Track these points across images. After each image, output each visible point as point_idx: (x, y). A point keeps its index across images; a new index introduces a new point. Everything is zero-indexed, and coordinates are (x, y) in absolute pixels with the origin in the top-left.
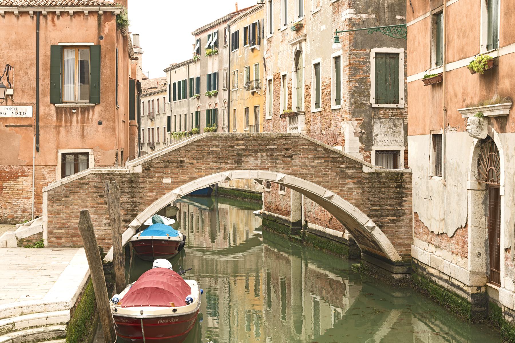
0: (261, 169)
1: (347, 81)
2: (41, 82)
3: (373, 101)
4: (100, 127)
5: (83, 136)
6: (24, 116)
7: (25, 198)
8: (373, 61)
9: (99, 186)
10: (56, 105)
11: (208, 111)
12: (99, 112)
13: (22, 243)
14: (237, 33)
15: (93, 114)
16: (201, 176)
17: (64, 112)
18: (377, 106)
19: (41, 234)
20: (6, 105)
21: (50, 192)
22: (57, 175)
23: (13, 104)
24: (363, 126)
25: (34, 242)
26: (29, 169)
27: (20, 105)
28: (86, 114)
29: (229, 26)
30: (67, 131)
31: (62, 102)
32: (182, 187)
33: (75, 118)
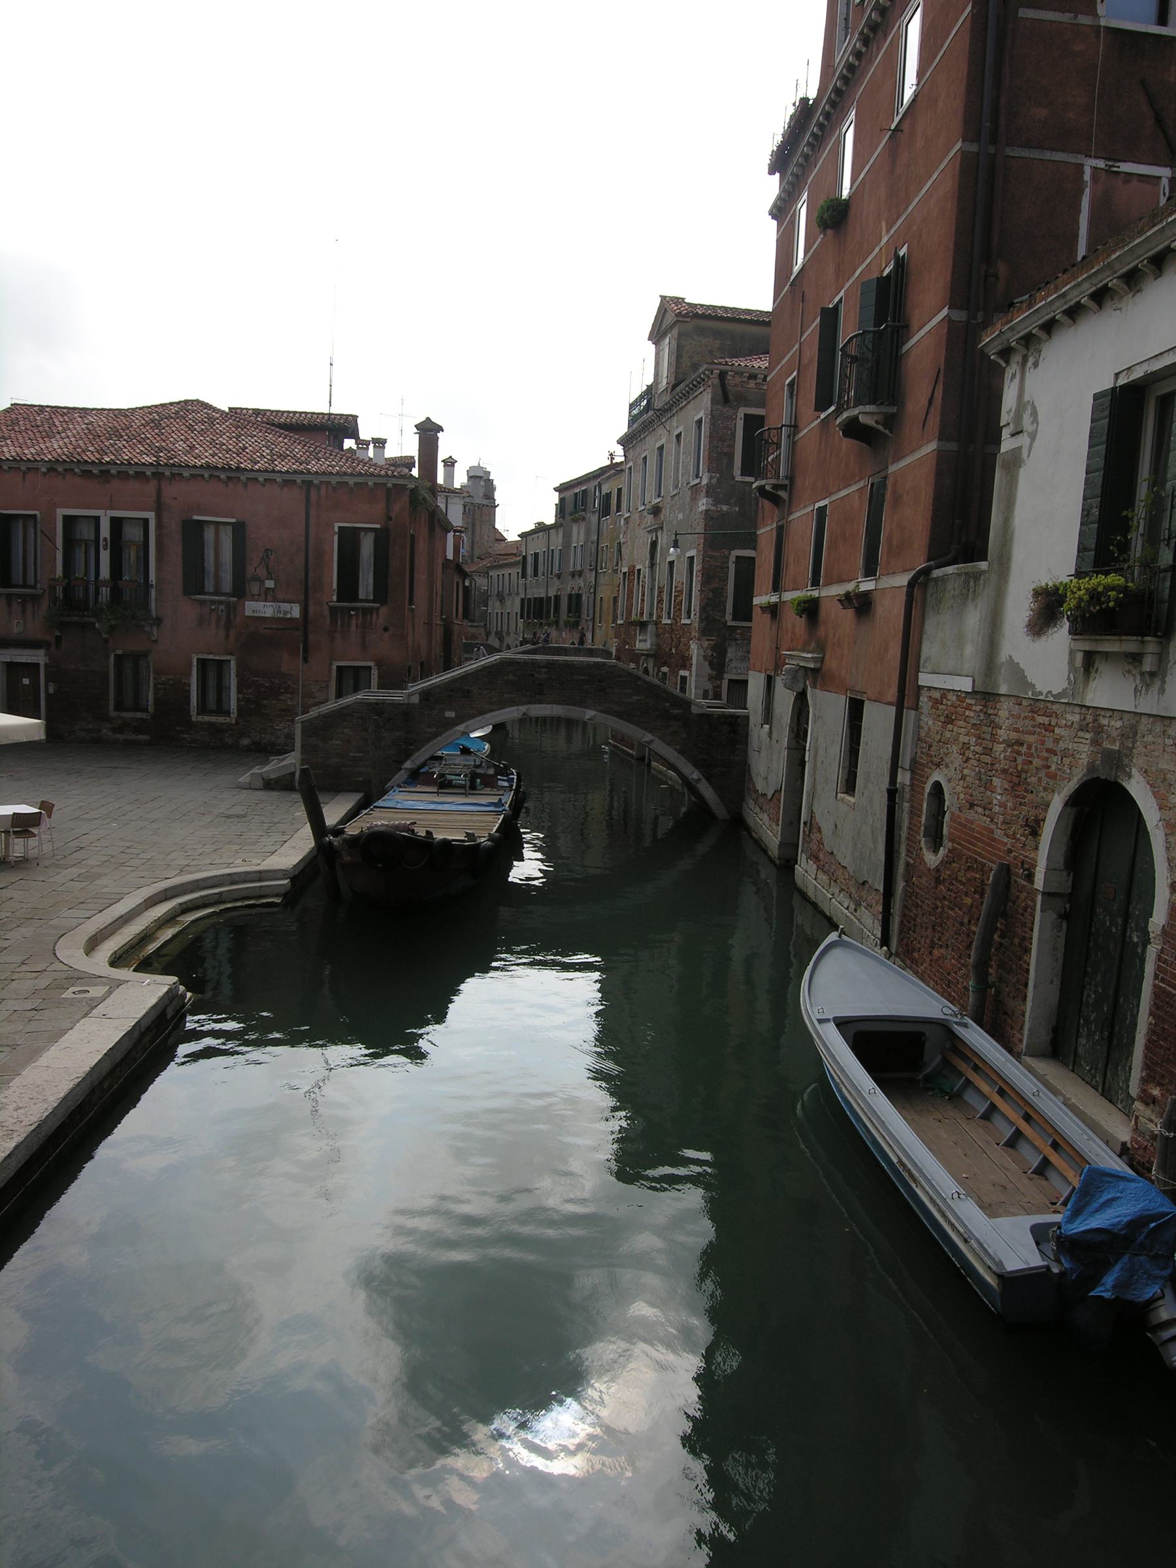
2: (310, 572)
3: (728, 617)
4: (386, 635)
8: (732, 567)
11: (570, 596)
14: (608, 495)
16: (492, 711)
18: (734, 624)
19: (293, 774)
20: (266, 601)
23: (275, 600)
24: (714, 648)
29: (600, 485)
33: (354, 621)
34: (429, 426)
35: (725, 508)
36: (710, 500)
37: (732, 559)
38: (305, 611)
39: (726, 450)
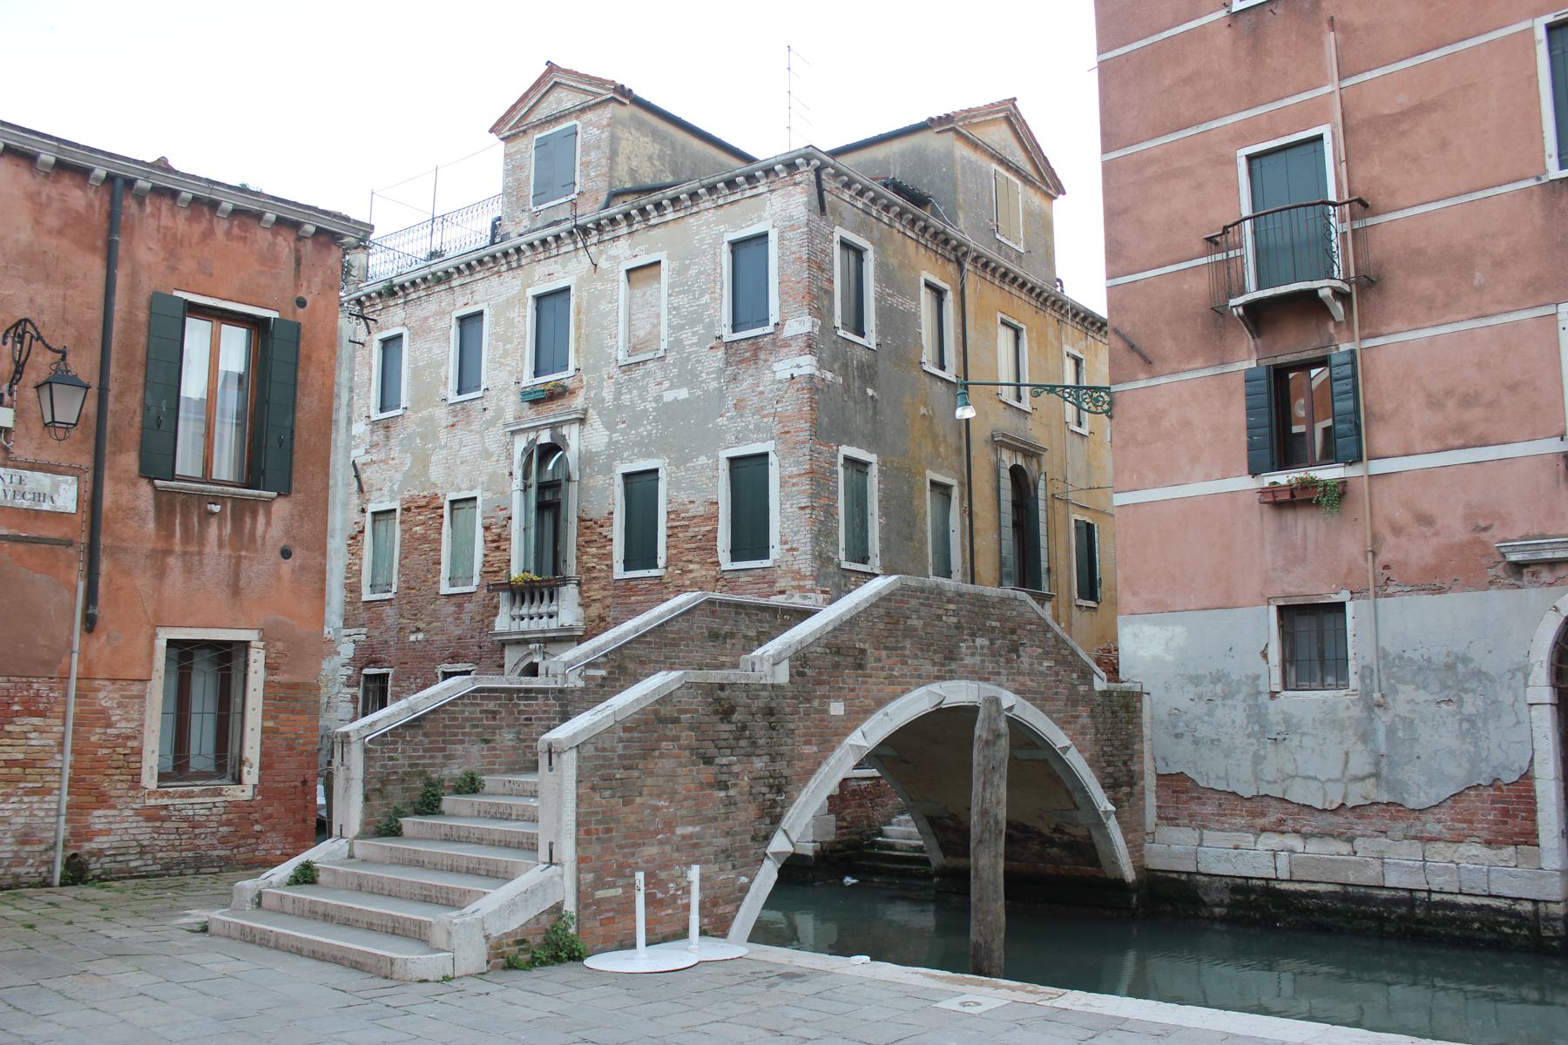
0: (980, 679)
2: (111, 404)
4: (287, 566)
5: (236, 590)
6: (46, 506)
8: (841, 471)
9: (703, 727)
10: (157, 482)
12: (284, 519)
15: (268, 523)
16: (894, 698)
17: (181, 507)
22: (148, 712)
25: (550, 947)
27: (33, 467)
28: (248, 520)
30: (188, 571)
32: (865, 726)
33: (213, 530)
35: (829, 376)
38: (93, 502)
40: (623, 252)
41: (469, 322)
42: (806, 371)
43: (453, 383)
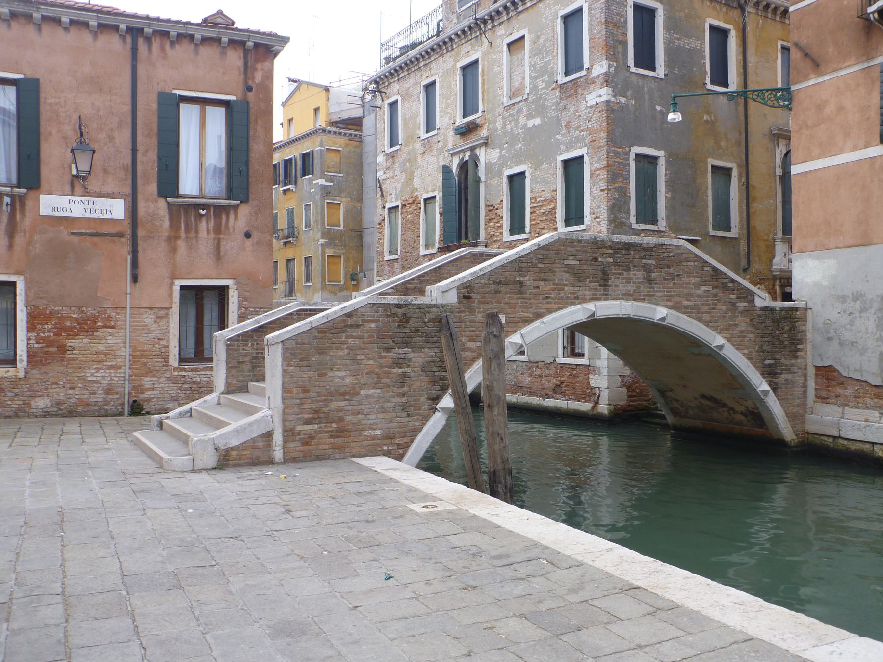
0: (635, 300)
1: (602, 191)
3: (633, 219)
4: (249, 243)
6: (107, 216)
7: (110, 368)
8: (633, 164)
13: (227, 460)
16: (550, 312)
19: (268, 435)
20: (72, 194)
21: (287, 345)
23: (87, 193)
26: (118, 314)
27: (100, 195)
28: (224, 217)
30: (190, 248)
31: (178, 196)
32: (524, 331)
33: (203, 225)
34: (219, 20)
36: (610, 90)
37: (632, 156)
39: (621, 37)
40: (504, 35)
41: (430, 87)
42: (604, 98)
43: (423, 127)
